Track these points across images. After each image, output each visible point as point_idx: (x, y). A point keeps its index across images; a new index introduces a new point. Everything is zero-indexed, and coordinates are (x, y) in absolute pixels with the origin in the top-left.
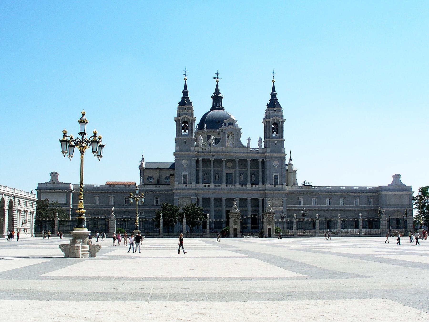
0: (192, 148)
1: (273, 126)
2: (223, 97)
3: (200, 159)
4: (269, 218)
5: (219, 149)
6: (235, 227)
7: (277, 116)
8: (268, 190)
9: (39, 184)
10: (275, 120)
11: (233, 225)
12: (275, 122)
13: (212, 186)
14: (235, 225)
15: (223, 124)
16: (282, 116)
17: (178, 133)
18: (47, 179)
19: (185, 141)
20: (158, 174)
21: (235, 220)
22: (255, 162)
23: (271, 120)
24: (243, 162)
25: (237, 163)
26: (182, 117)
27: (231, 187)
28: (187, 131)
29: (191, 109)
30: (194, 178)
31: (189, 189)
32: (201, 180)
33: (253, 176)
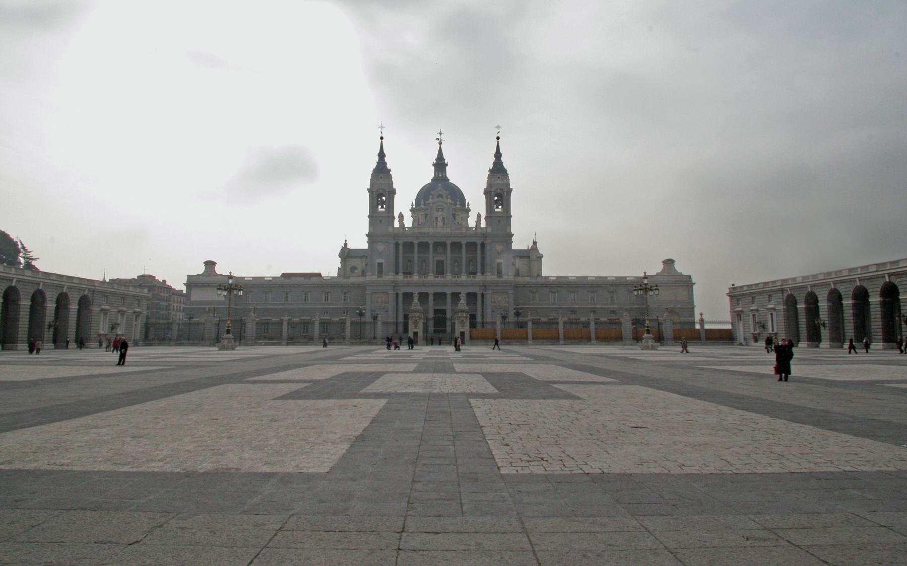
0: (390, 229)
1: (496, 198)
2: (447, 165)
3: (401, 242)
6: (416, 330)
9: (189, 277)
11: (413, 328)
13: (416, 277)
14: (416, 327)
15: (431, 197)
16: (508, 184)
18: (201, 269)
19: (380, 219)
22: (472, 246)
24: (456, 246)
25: (449, 247)
33: (471, 264)
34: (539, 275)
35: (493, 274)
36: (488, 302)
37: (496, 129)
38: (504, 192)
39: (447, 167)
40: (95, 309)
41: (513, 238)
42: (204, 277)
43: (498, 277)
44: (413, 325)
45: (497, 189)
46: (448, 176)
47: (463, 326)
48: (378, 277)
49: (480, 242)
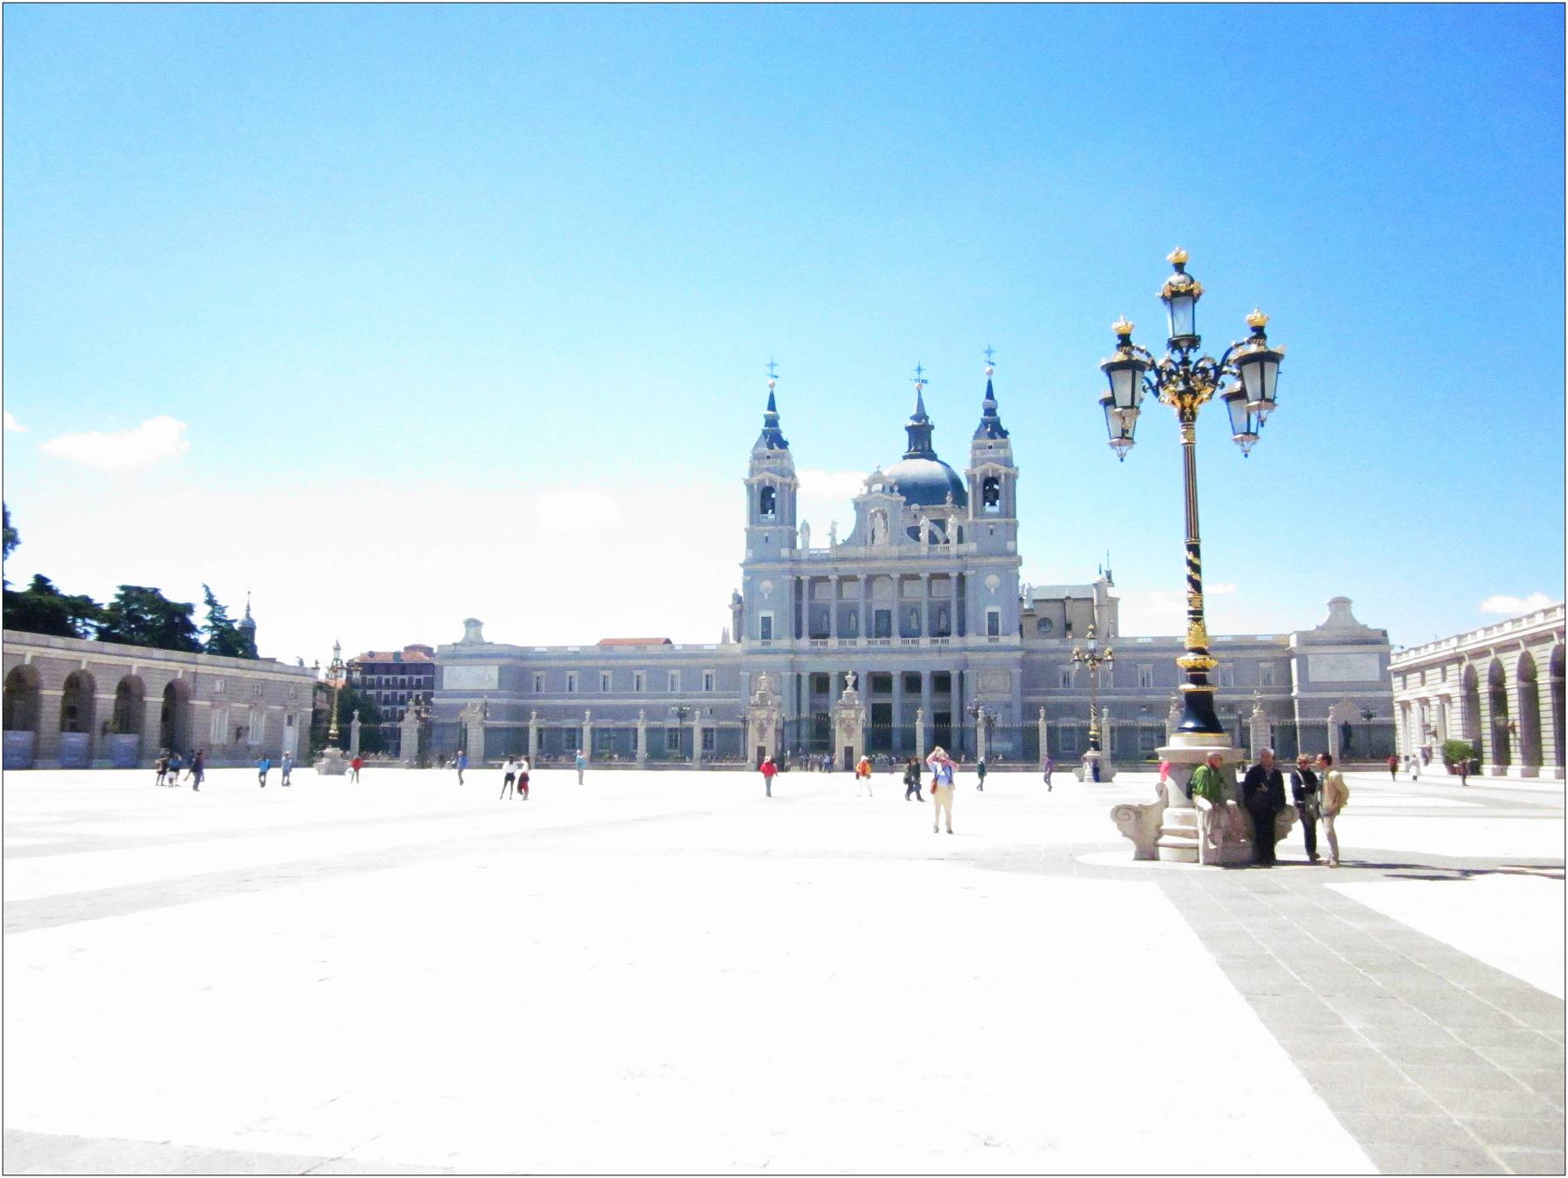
0: (785, 553)
4: (846, 722)
6: (761, 744)
7: (996, 461)
8: (973, 650)
10: (990, 471)
12: (990, 476)
13: (833, 642)
16: (1008, 462)
17: (753, 520)
19: (766, 534)
21: (761, 725)
26: (760, 477)
27: (879, 646)
30: (789, 626)
31: (775, 652)
35: (980, 634)
36: (970, 687)
37: (986, 355)
38: (1000, 477)
40: (199, 703)
42: (465, 648)
43: (990, 640)
44: (757, 735)
45: (987, 470)
46: (933, 448)
47: (849, 737)
48: (763, 644)
49: (956, 574)
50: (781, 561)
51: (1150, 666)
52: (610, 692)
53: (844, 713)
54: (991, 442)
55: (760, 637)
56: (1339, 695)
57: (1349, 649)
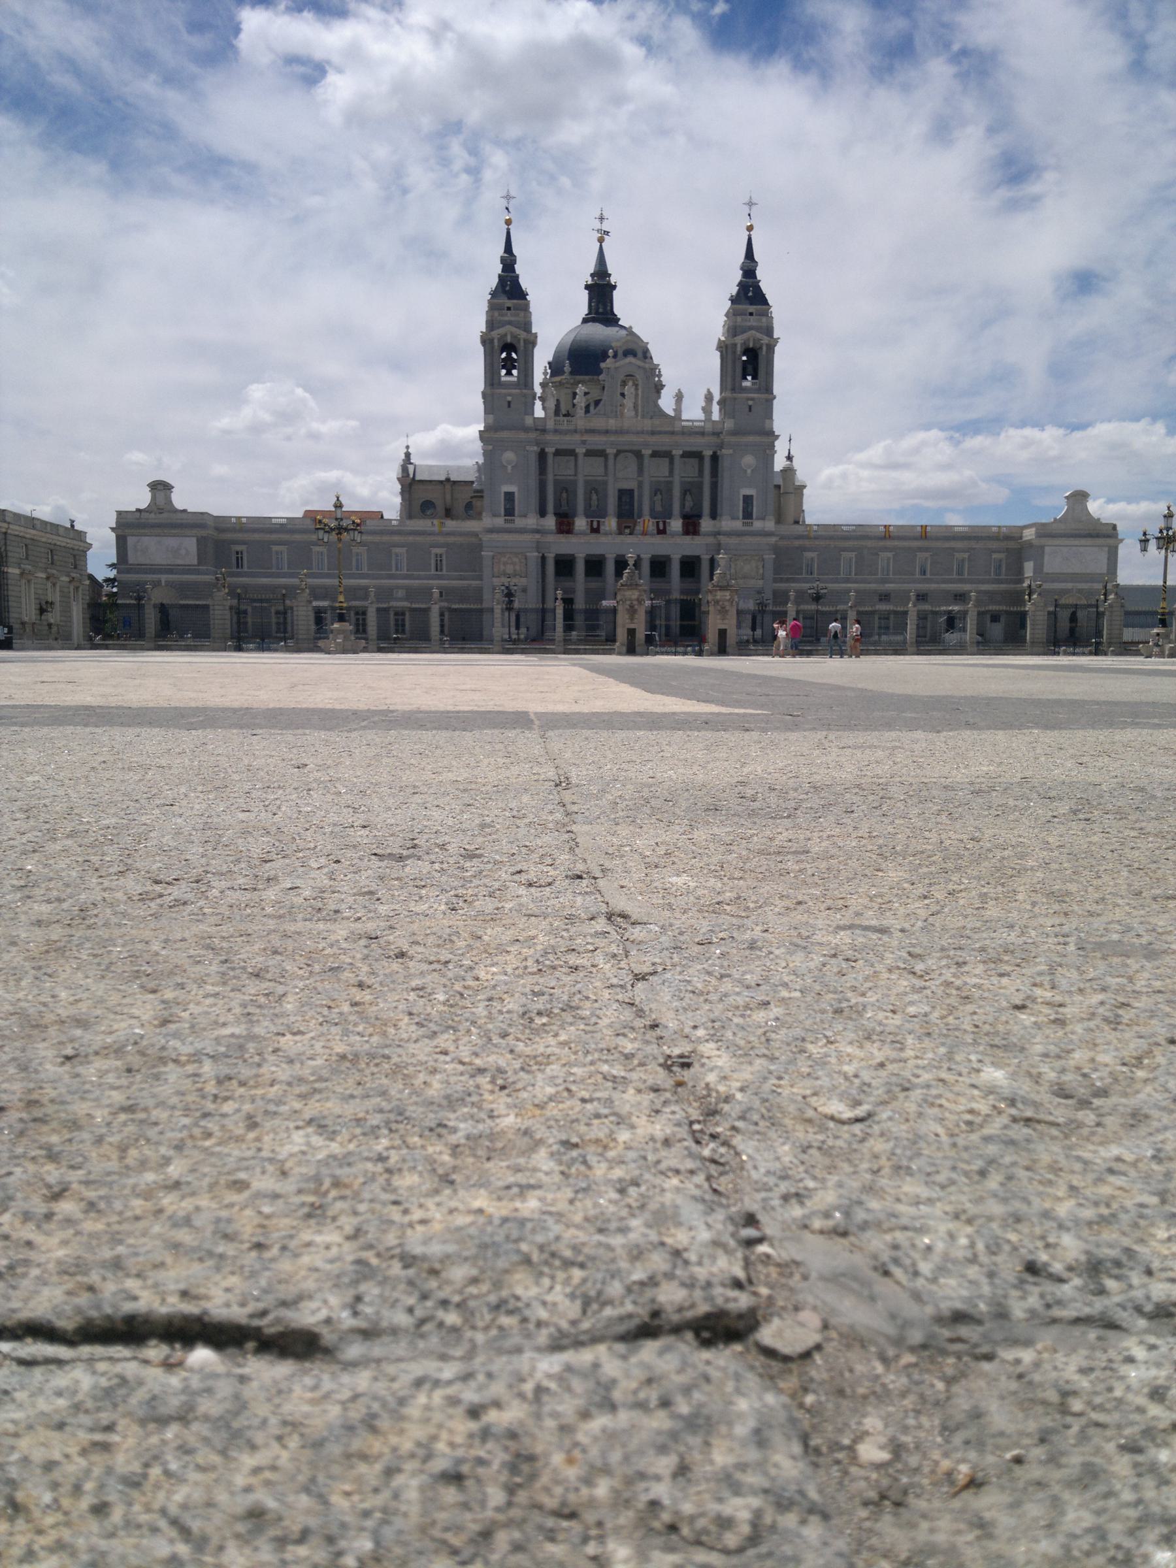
0: (529, 421)
2: (614, 287)
5: (598, 423)
6: (632, 626)
7: (758, 329)
9: (119, 513)
14: (632, 619)
16: (769, 331)
17: (491, 379)
18: (141, 499)
20: (448, 497)
21: (632, 606)
23: (739, 340)
25: (646, 461)
26: (502, 331)
28: (515, 372)
29: (526, 308)
32: (550, 507)
33: (688, 497)
34: (797, 522)
35: (734, 518)
39: (615, 293)
41: (777, 443)
46: (616, 311)
50: (526, 430)
51: (890, 555)
52: (365, 571)
53: (719, 595)
54: (752, 309)
55: (502, 512)
56: (1069, 586)
57: (1083, 541)
